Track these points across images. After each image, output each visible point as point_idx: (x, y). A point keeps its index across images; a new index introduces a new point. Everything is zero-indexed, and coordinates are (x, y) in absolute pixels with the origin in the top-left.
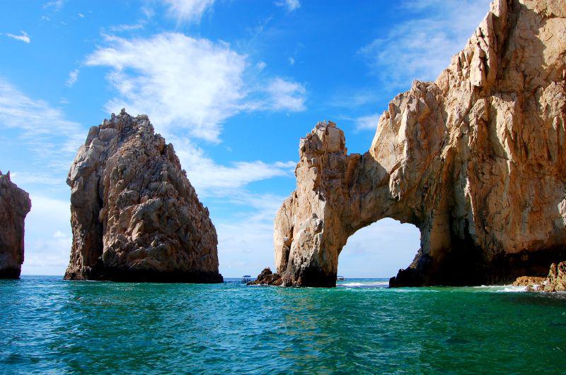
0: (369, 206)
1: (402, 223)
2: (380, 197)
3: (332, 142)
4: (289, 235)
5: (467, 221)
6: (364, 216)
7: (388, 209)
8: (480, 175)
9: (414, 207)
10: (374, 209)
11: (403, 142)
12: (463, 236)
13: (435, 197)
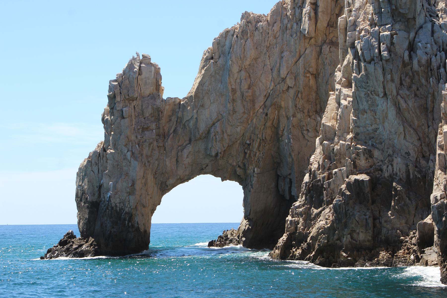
0: (187, 161)
1: (222, 180)
2: (199, 152)
3: (146, 84)
4: (97, 194)
5: (290, 180)
6: (181, 172)
7: (207, 166)
8: (305, 132)
9: (235, 164)
10: (192, 165)
12: (288, 198)
13: (257, 154)
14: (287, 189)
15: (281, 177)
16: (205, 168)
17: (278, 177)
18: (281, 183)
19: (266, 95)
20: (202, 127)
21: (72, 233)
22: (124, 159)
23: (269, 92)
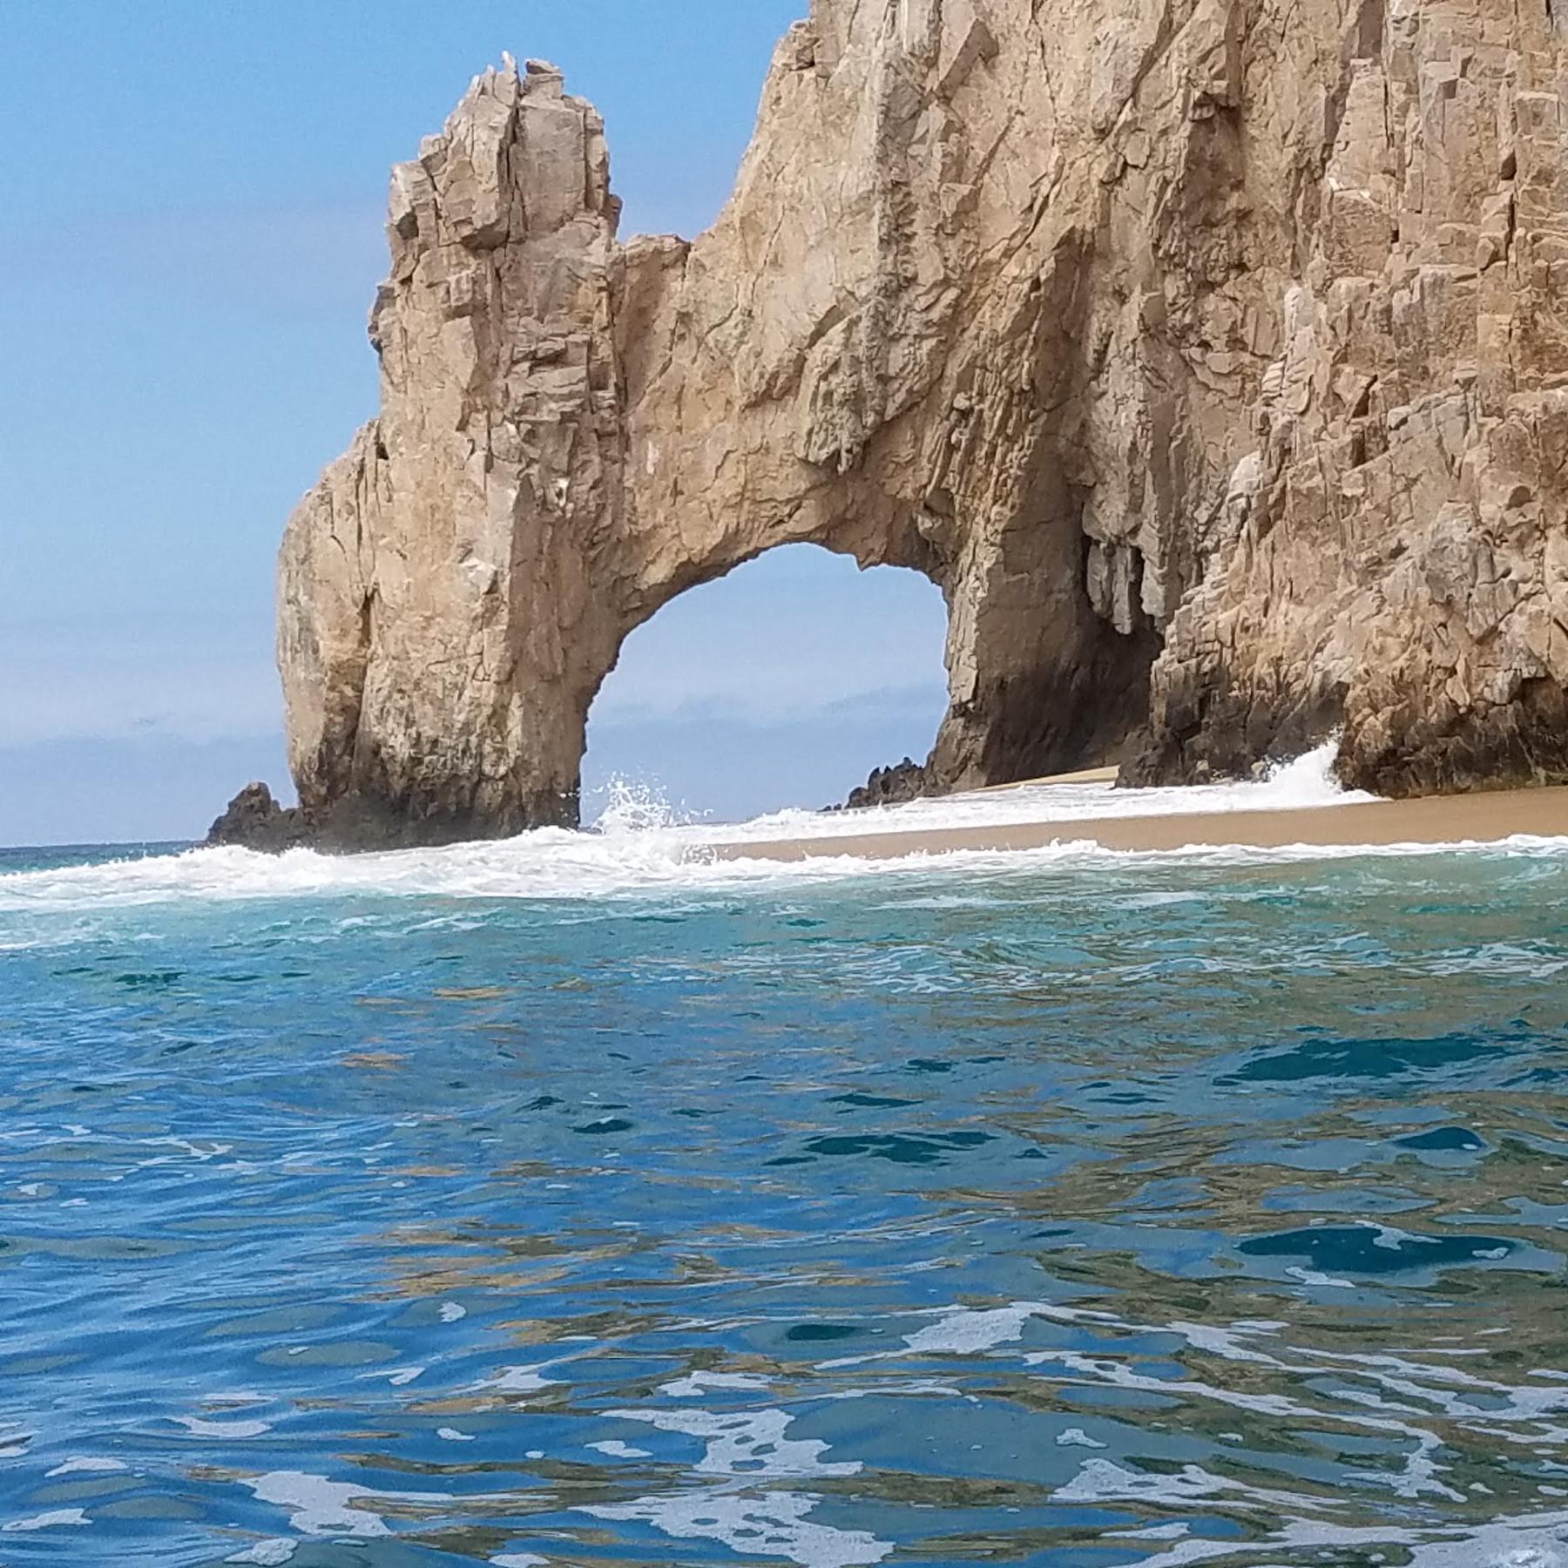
1: (862, 565)
2: (764, 449)
4: (355, 633)
5: (1137, 552)
7: (798, 508)
8: (1195, 353)
9: (908, 492)
11: (866, 197)
12: (1124, 626)
13: (999, 450)
14: (1122, 590)
15: (1098, 543)
16: (790, 516)
17: (1087, 543)
18: (1098, 570)
19: (1031, 207)
20: (776, 351)
21: (262, 791)
22: (460, 483)
23: (1044, 190)
